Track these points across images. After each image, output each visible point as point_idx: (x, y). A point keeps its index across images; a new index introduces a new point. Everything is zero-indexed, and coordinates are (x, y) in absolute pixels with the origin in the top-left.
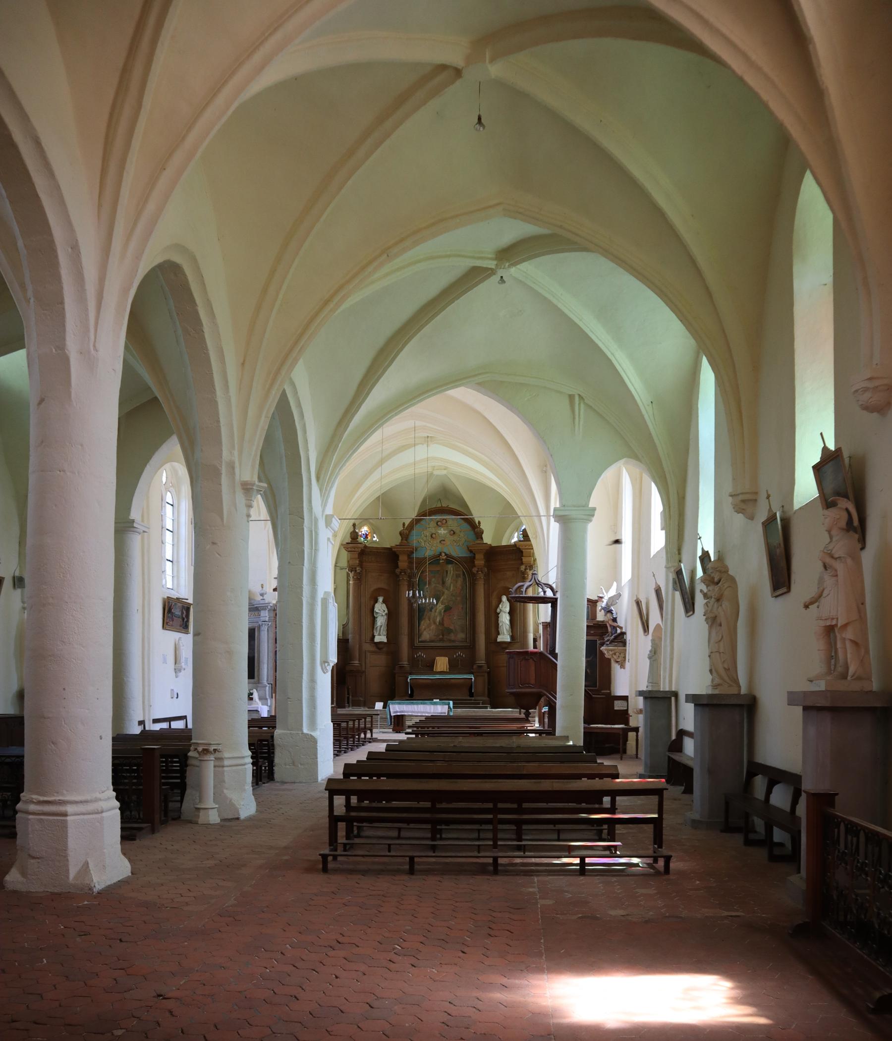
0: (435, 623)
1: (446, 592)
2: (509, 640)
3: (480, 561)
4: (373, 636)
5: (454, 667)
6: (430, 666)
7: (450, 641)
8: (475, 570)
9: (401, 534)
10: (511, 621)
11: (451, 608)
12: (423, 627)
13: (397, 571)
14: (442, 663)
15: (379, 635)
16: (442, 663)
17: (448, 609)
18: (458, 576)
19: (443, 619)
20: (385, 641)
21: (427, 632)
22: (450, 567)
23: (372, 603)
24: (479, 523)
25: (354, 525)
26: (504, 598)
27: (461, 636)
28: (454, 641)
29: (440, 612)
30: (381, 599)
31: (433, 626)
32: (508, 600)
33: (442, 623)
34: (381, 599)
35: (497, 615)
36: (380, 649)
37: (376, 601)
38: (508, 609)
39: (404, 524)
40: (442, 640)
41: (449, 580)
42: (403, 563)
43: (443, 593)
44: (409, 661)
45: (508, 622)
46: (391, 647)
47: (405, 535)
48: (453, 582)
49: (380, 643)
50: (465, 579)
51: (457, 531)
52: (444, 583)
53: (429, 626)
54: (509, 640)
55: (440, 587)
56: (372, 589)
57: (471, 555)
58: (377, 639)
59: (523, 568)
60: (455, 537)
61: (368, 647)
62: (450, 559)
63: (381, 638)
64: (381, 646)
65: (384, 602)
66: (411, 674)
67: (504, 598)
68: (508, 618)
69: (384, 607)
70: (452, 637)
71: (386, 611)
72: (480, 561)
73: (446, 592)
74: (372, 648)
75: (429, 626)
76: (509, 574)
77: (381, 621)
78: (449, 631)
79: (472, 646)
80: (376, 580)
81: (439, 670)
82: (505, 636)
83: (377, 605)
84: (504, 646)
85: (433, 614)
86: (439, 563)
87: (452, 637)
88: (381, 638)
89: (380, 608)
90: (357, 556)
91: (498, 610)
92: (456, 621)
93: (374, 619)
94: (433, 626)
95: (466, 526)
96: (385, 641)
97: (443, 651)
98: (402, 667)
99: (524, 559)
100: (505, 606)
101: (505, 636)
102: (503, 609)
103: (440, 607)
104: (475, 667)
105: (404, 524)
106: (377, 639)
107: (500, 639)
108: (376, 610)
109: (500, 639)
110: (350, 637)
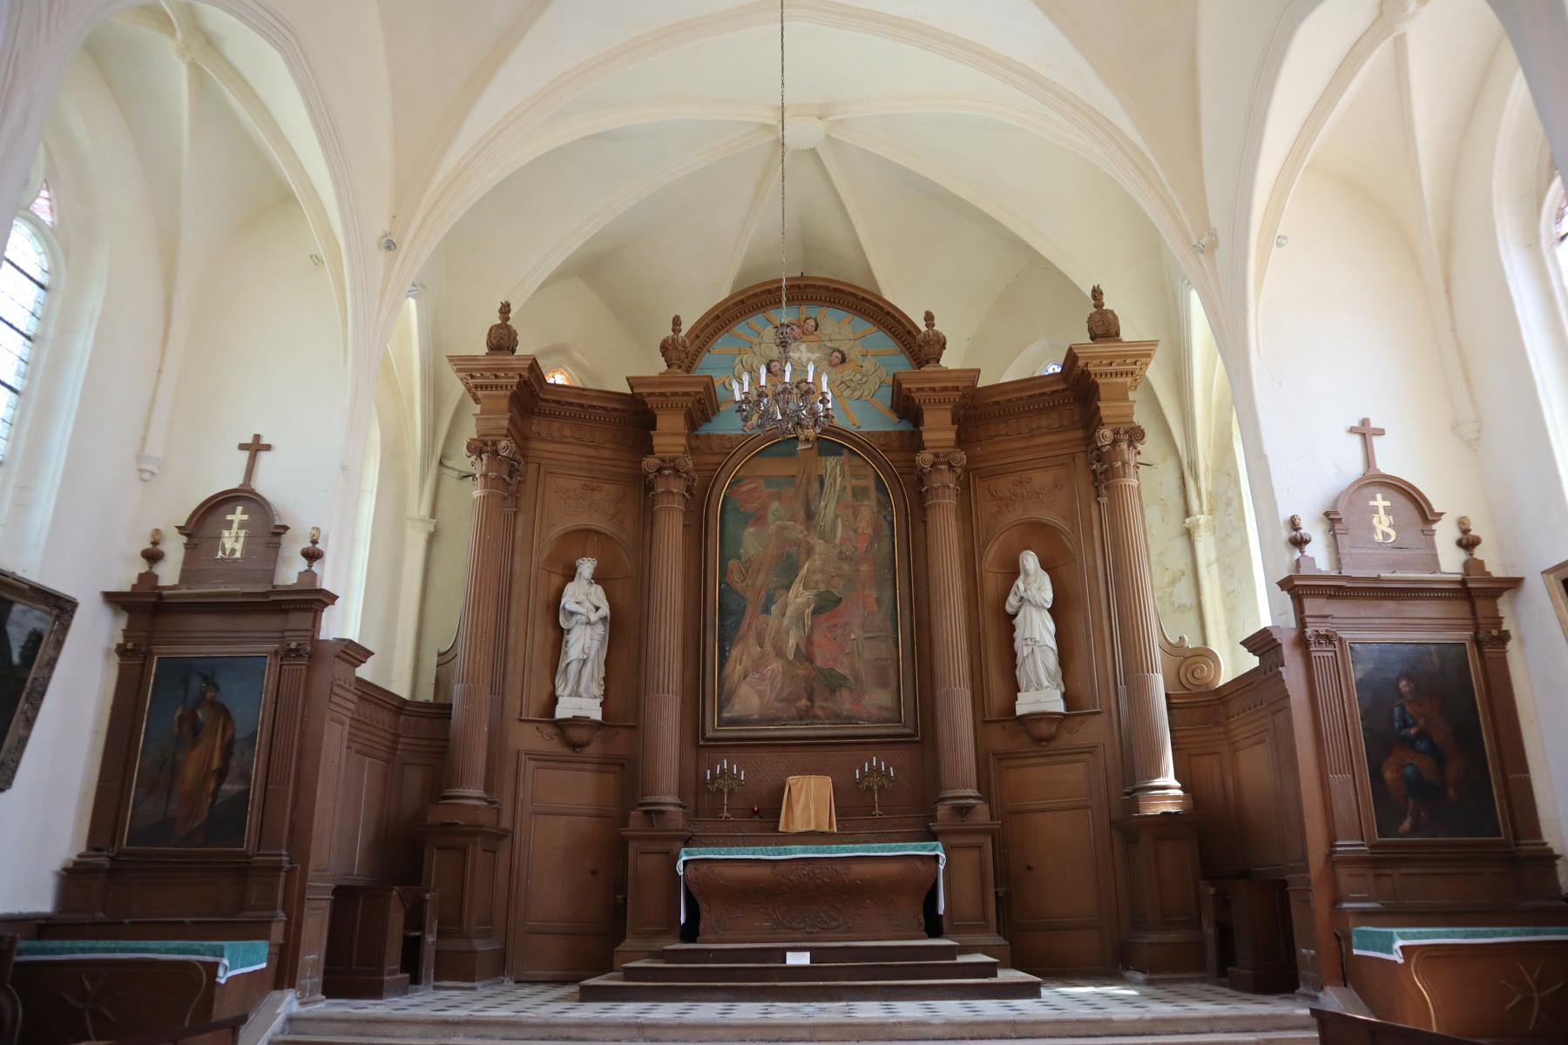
0: (780, 653)
1: (820, 546)
2: (1060, 707)
3: (939, 430)
4: (554, 700)
5: (854, 812)
6: (765, 814)
7: (836, 717)
8: (924, 458)
9: (665, 348)
10: (1063, 638)
11: (840, 600)
12: (735, 669)
13: (649, 463)
14: (810, 800)
15: (576, 693)
16: (810, 800)
17: (826, 605)
18: (859, 493)
19: (809, 641)
20: (596, 714)
21: (754, 688)
22: (831, 464)
23: (556, 580)
24: (929, 318)
25: (505, 309)
26: (1030, 561)
27: (878, 699)
28: (850, 719)
29: (800, 617)
30: (586, 567)
31: (775, 666)
32: (1046, 565)
33: (805, 654)
34: (586, 567)
35: (1008, 622)
36: (575, 746)
37: (570, 574)
38: (1048, 595)
39: (677, 322)
40: (805, 716)
41: (828, 508)
42: (670, 435)
43: (810, 552)
44: (681, 794)
45: (1052, 643)
46: (617, 739)
47: (682, 351)
48: (845, 516)
49: (576, 722)
50: (884, 503)
51: (854, 354)
52: (810, 516)
53: (759, 664)
54: (1060, 707)
55: (797, 530)
56: (558, 530)
57: (905, 426)
58: (564, 710)
59: (1106, 434)
60: (847, 373)
61: (528, 738)
62: (832, 442)
63: (580, 702)
64: (578, 734)
65: (598, 578)
66: (688, 842)
67: (1030, 561)
68: (1052, 627)
69: (598, 594)
70: (845, 702)
71: (605, 610)
72: (939, 430)
73: (820, 546)
74: (553, 746)
75: (759, 664)
76: (1041, 479)
77: (585, 643)
78: (834, 683)
79: (919, 735)
80: (571, 500)
81: (799, 826)
82: (1041, 695)
83: (570, 588)
84: (1045, 729)
85: (772, 620)
86: (792, 454)
87: (845, 702)
88: (580, 702)
89: (584, 599)
90: (505, 404)
91: (1012, 601)
92: (861, 643)
93: (560, 635)
94: (775, 666)
95: (881, 341)
96: (596, 714)
97: (812, 750)
98: (653, 814)
99: (1106, 409)
100: (1036, 585)
101: (1041, 695)
102: (1033, 594)
103: (799, 597)
104: (942, 810)
105: (677, 322)
106: (564, 710)
107: (1025, 704)
108: (568, 602)
109: (1025, 704)
110: (457, 691)
